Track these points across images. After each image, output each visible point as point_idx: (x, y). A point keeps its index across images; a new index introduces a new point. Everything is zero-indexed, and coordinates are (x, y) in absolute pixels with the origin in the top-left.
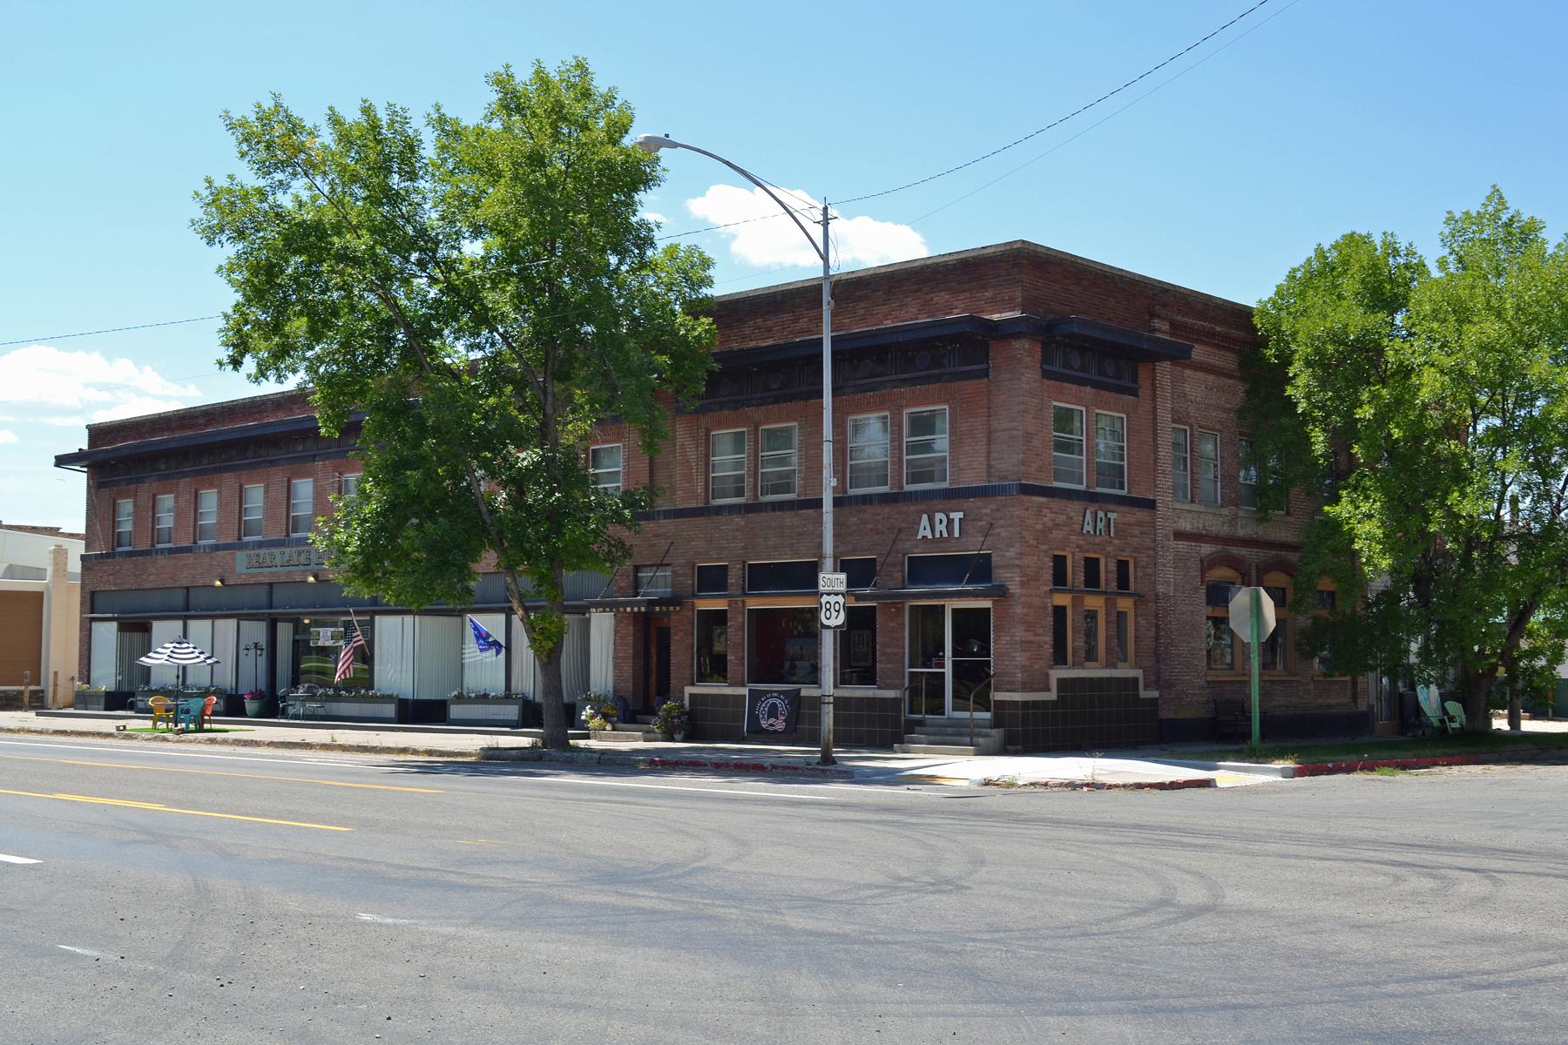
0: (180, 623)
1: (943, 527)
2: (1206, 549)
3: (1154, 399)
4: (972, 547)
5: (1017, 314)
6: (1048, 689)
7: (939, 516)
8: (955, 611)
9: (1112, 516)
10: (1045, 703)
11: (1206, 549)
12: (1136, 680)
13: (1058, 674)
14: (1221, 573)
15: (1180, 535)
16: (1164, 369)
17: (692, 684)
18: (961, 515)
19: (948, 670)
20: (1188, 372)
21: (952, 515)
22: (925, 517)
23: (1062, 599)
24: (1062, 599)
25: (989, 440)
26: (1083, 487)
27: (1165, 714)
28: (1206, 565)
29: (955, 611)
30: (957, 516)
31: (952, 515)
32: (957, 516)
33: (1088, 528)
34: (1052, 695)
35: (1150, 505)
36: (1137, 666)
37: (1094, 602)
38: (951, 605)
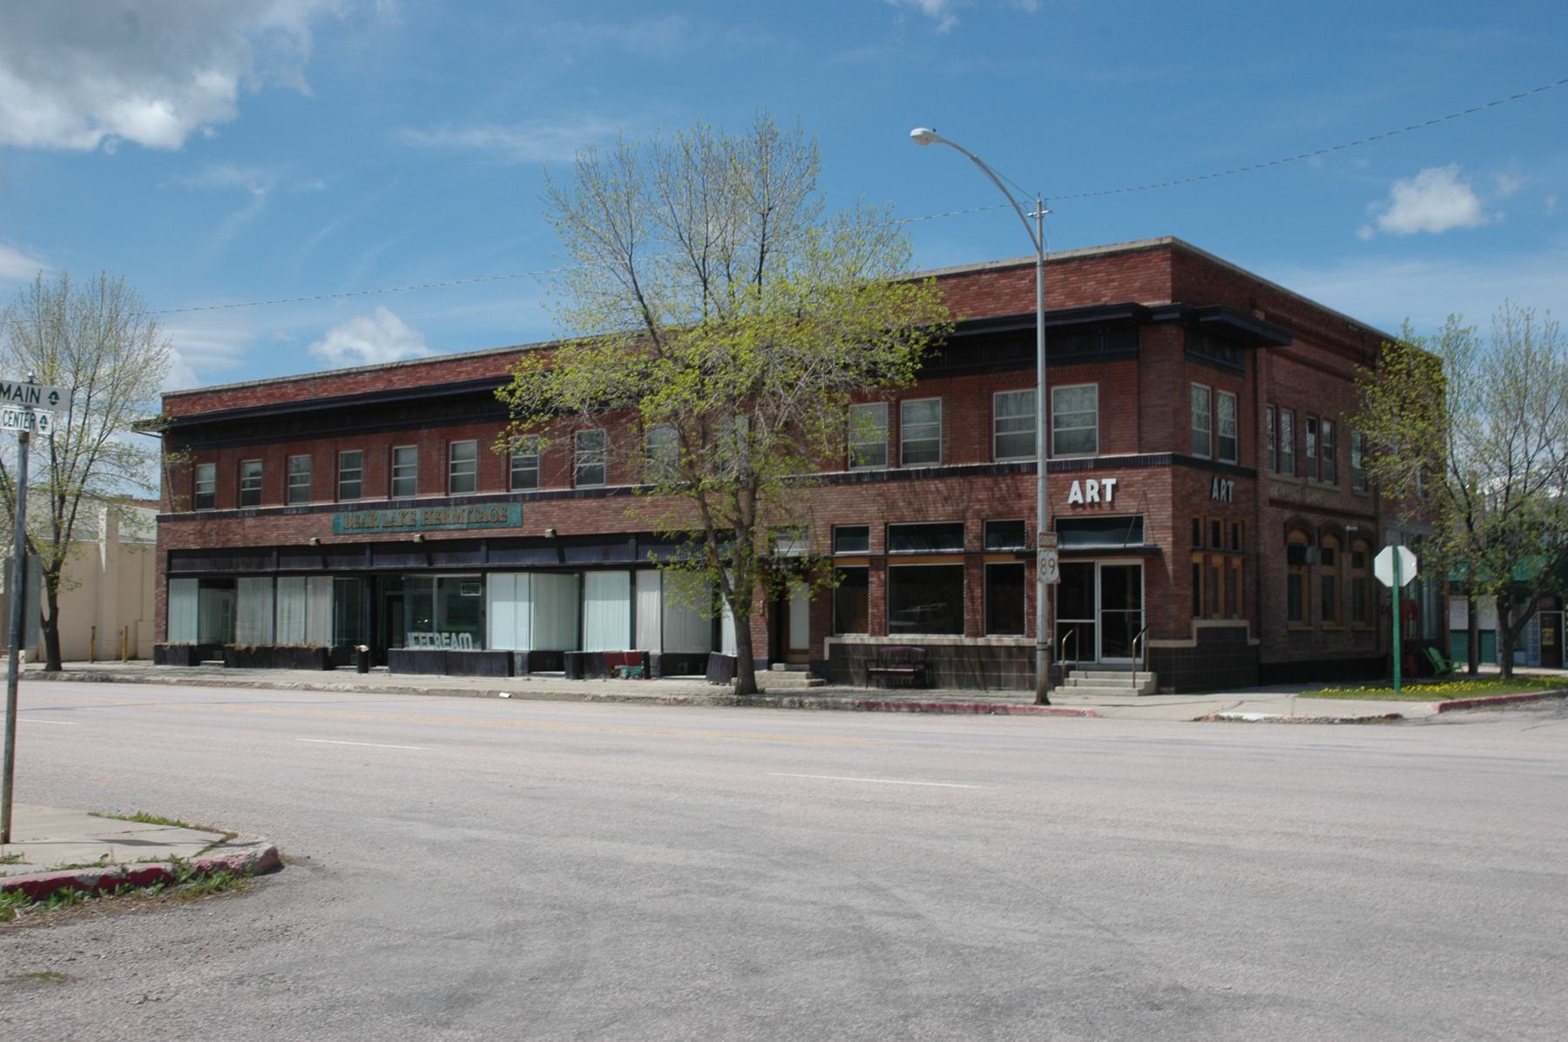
0: (626, 575)
1: (1223, 492)
2: (1288, 514)
3: (1255, 379)
4: (1128, 507)
5: (1168, 302)
6: (1190, 637)
7: (1090, 482)
8: (1105, 570)
9: (1231, 484)
10: (1189, 649)
11: (1288, 514)
12: (1245, 629)
13: (1198, 623)
14: (1297, 536)
15: (1273, 502)
16: (1262, 353)
17: (831, 635)
18: (1113, 481)
19: (1098, 621)
20: (1275, 358)
21: (1104, 481)
22: (1076, 484)
23: (1198, 558)
24: (1198, 558)
25: (1140, 417)
26: (1208, 458)
27: (1266, 659)
28: (1288, 527)
29: (1105, 570)
30: (1109, 482)
31: (1104, 481)
32: (1109, 482)
33: (1215, 494)
34: (1192, 643)
35: (1253, 475)
36: (1243, 617)
37: (1217, 560)
38: (1100, 563)
